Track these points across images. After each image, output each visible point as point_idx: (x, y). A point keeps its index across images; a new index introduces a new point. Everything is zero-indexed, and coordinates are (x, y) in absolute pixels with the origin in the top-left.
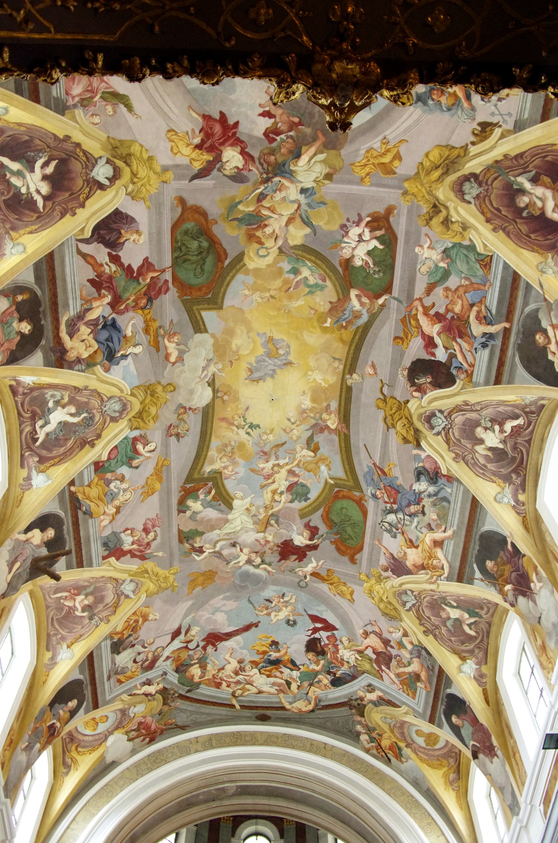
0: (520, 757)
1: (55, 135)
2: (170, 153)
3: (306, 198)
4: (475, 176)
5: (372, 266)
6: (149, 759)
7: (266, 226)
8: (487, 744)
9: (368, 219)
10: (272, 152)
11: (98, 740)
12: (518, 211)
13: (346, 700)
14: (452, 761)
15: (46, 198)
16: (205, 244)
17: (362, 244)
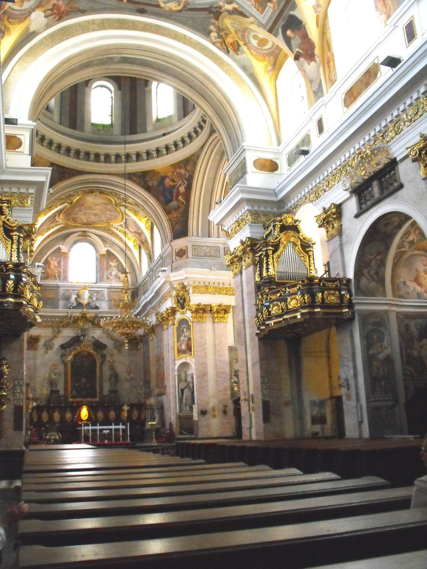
0: (334, 64)
6: (59, 32)
8: (310, 52)
11: (24, 14)
13: (208, 6)
14: (272, 58)
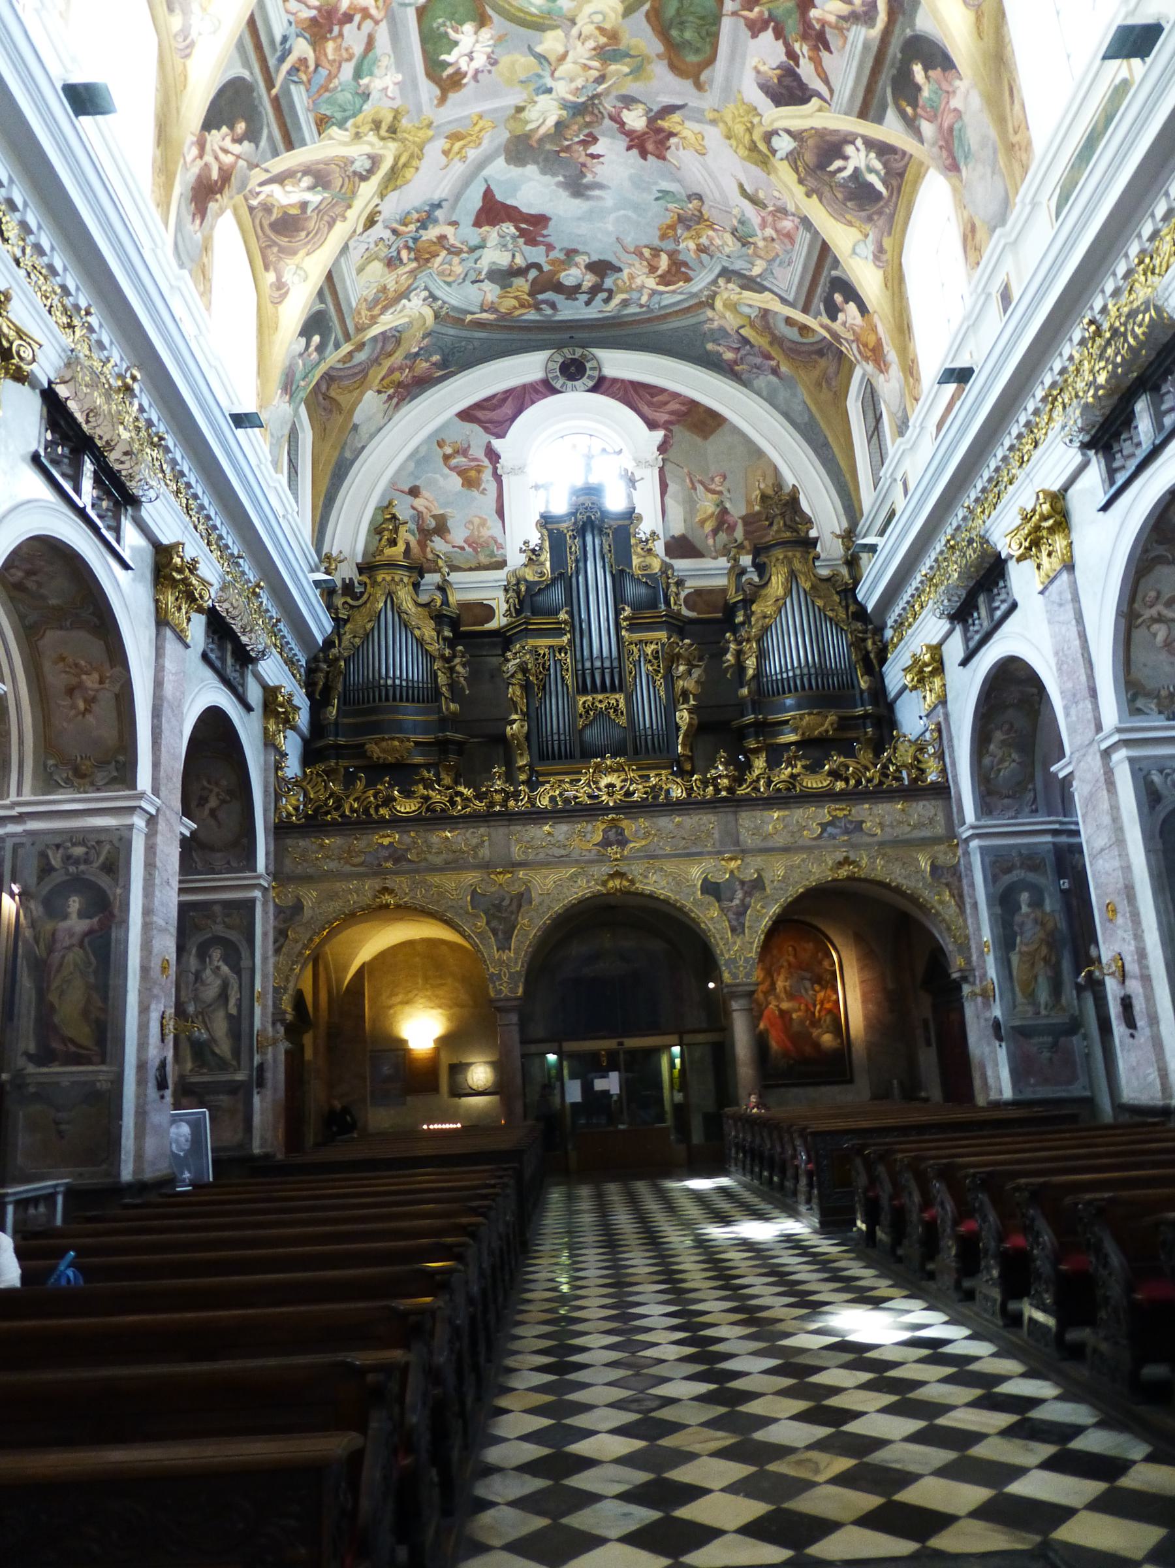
1: (820, 200)
2: (705, 134)
3: (545, 84)
4: (364, 178)
5: (450, 31)
7: (594, 49)
9: (465, 81)
10: (588, 125)
12: (306, 172)
15: (853, 143)
16: (674, 33)
17: (467, 51)
